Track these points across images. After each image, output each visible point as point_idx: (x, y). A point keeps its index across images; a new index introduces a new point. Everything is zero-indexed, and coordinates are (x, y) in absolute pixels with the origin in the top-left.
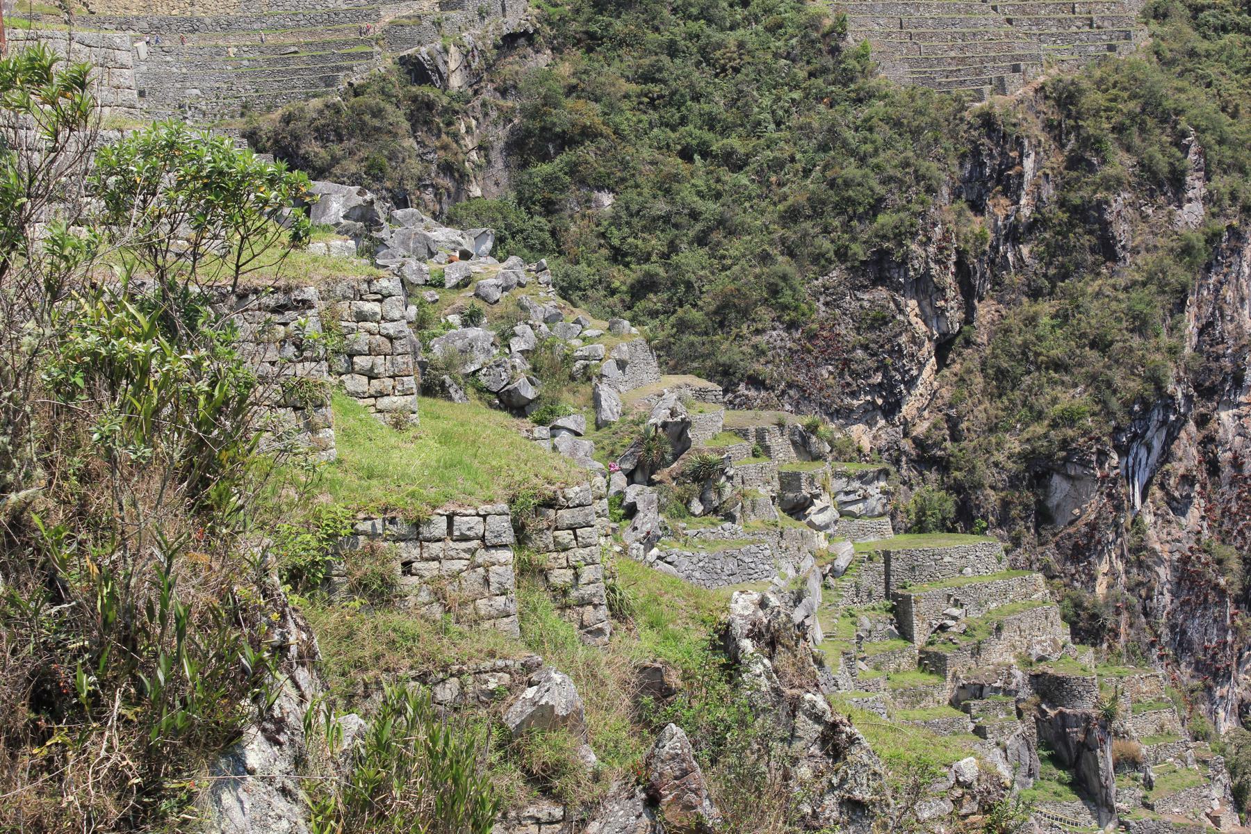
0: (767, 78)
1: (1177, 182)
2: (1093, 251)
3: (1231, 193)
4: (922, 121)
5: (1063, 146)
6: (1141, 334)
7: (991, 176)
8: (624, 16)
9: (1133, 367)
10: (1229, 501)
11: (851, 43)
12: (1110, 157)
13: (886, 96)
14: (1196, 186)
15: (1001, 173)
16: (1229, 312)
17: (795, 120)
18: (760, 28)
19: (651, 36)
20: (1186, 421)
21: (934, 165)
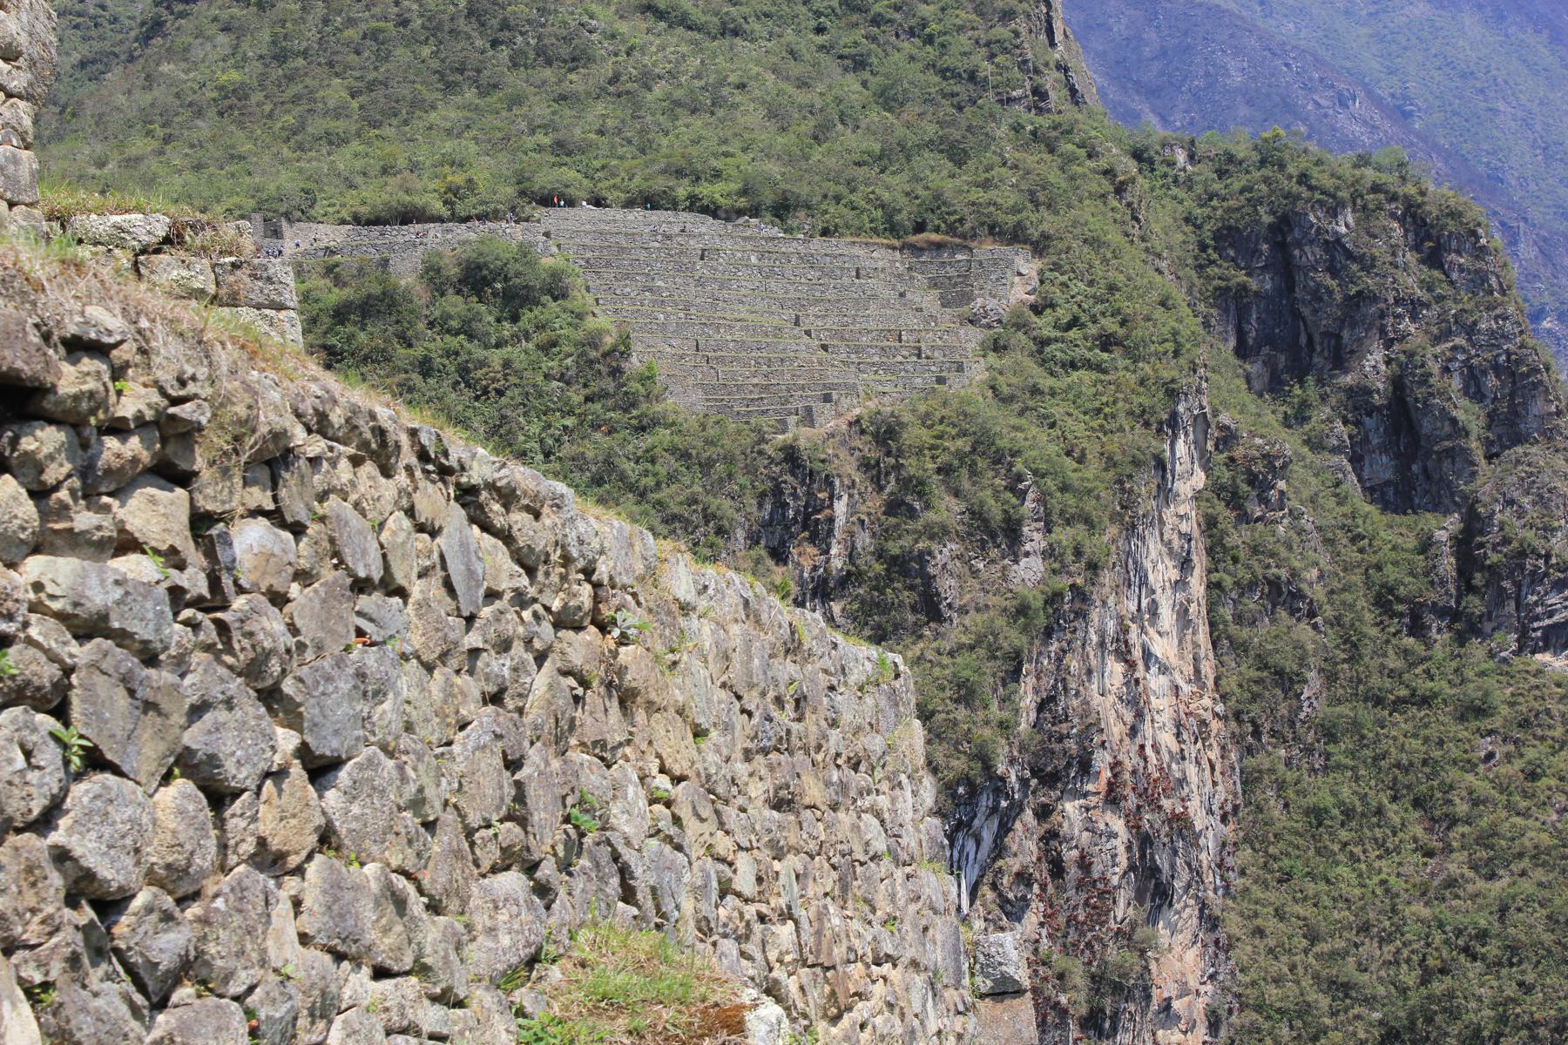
0: (536, 403)
1: (1012, 531)
2: (914, 609)
3: (1076, 548)
4: (711, 452)
5: (881, 489)
6: (967, 705)
7: (795, 519)
8: (369, 328)
9: (958, 742)
10: (1075, 907)
11: (634, 364)
12: (935, 502)
13: (673, 424)
14: (1034, 539)
15: (807, 517)
16: (1074, 686)
17: (567, 450)
18: (531, 346)
19: (402, 351)
20: (1022, 810)
21: (727, 503)
